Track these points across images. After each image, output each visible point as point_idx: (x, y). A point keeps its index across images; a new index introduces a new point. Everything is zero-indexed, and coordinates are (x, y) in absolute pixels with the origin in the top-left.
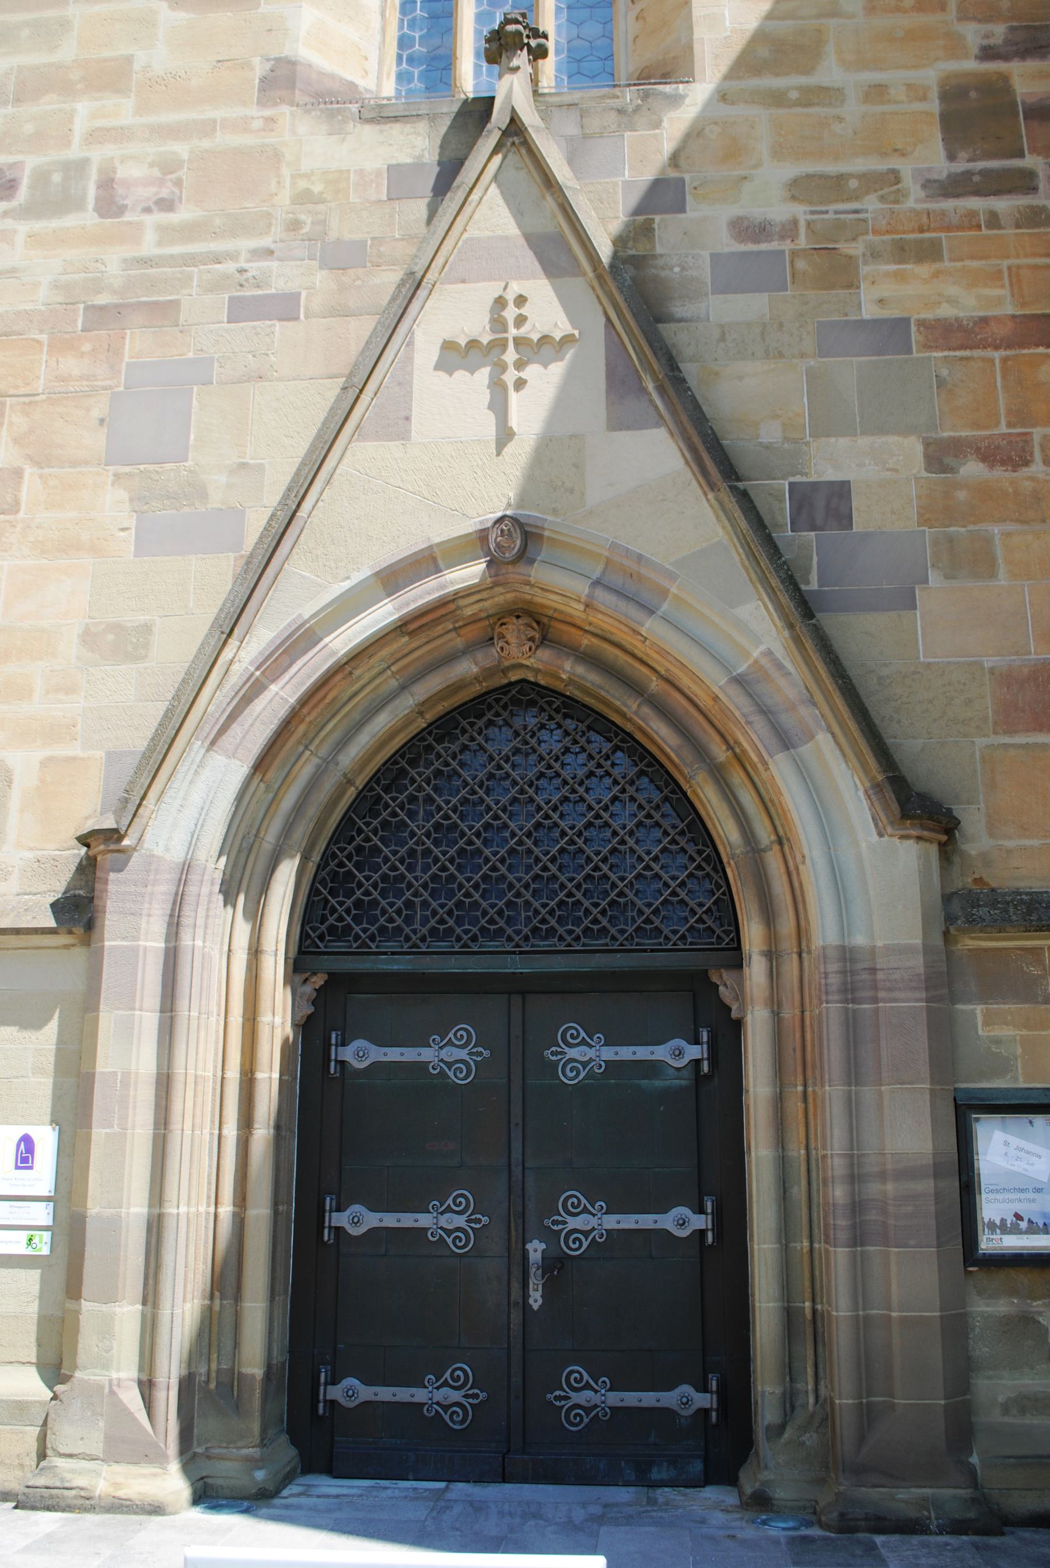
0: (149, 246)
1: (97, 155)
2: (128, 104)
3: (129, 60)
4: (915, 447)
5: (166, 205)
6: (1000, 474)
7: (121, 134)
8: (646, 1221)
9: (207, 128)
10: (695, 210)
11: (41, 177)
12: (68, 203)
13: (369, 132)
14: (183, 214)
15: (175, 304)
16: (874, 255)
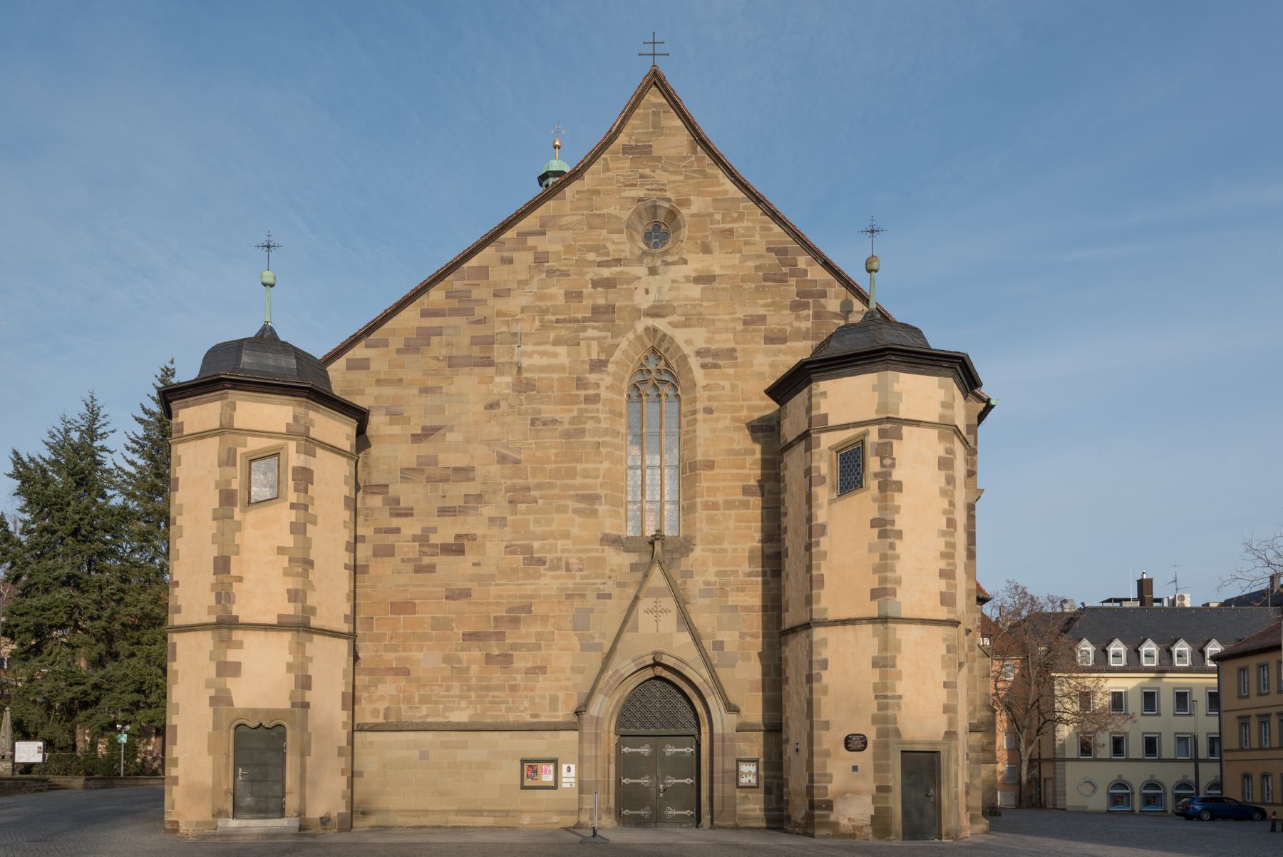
0: (578, 580)
1: (565, 555)
2: (570, 542)
3: (569, 531)
4: (737, 634)
5: (581, 570)
6: (754, 640)
7: (568, 551)
8: (682, 781)
9: (589, 551)
10: (696, 578)
11: (552, 561)
12: (558, 568)
13: (626, 554)
15: (585, 595)
16: (732, 590)
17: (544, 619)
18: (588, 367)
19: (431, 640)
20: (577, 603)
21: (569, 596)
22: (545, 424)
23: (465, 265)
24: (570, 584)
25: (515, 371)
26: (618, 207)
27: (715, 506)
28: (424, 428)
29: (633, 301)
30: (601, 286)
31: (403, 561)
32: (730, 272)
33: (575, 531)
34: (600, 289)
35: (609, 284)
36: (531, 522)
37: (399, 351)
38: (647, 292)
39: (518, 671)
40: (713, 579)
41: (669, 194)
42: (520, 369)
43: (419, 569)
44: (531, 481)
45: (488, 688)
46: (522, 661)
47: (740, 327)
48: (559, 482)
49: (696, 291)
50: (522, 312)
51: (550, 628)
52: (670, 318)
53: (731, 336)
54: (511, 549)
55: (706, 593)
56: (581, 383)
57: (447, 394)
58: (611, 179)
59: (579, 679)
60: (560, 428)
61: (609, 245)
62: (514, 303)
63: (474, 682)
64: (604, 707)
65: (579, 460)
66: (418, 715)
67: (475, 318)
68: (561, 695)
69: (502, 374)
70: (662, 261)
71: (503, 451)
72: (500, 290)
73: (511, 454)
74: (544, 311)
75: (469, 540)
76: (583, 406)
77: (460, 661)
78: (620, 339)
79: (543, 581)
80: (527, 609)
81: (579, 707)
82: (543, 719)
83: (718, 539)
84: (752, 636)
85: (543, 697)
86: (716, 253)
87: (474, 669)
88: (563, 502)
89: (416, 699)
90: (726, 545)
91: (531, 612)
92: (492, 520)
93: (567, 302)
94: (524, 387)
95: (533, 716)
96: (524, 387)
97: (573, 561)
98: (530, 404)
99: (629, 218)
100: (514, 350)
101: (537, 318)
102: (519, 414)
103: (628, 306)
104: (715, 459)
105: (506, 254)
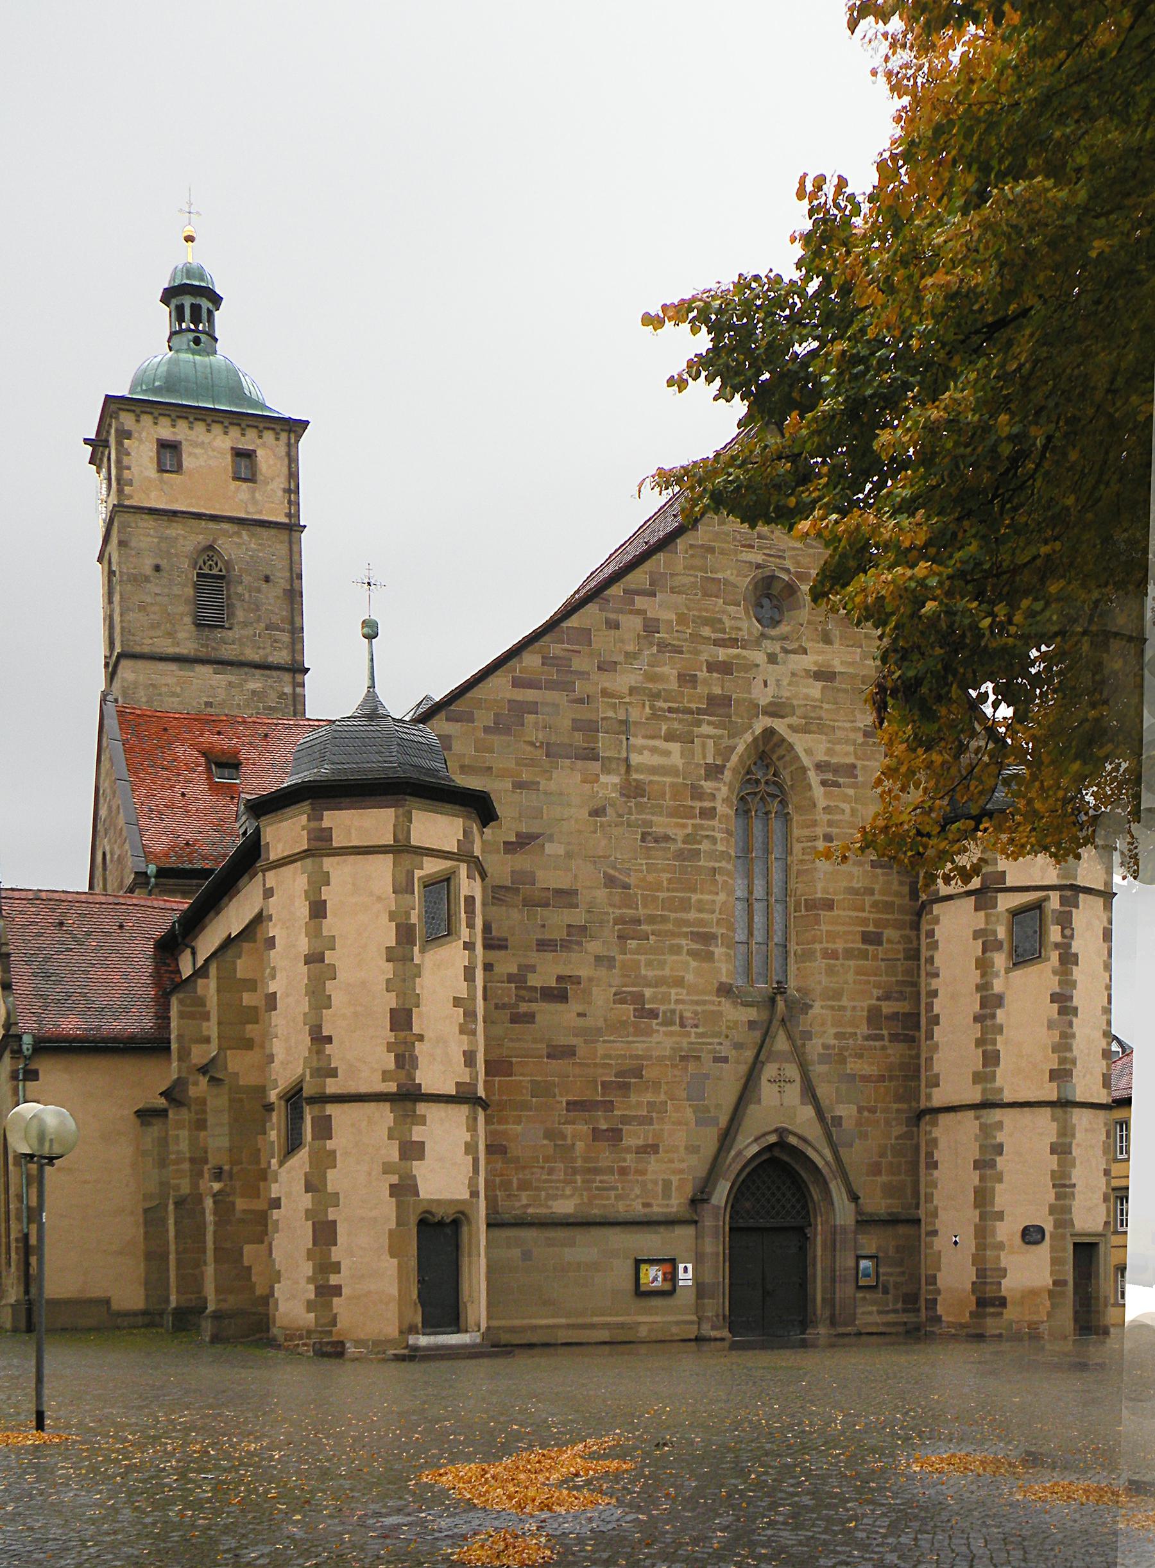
2: (685, 992)
4: (855, 1107)
5: (696, 1026)
9: (704, 1002)
11: (665, 1013)
12: (672, 1023)
14: (700, 1030)
16: (850, 1055)
17: (656, 1085)
18: (703, 772)
19: (530, 1110)
20: (691, 1066)
21: (683, 1058)
22: (656, 841)
23: (564, 625)
24: (685, 1042)
25: (623, 770)
26: (735, 572)
27: (834, 955)
28: (518, 835)
29: (750, 693)
30: (718, 671)
31: (497, 1007)
32: (851, 670)
33: (690, 977)
34: (715, 675)
35: (724, 668)
36: (643, 964)
37: (487, 730)
38: (766, 685)
39: (628, 1150)
40: (833, 1042)
41: (788, 564)
42: (628, 767)
43: (516, 1019)
44: (642, 912)
45: (596, 1171)
46: (633, 1138)
47: (860, 740)
48: (673, 915)
49: (815, 690)
50: (630, 695)
51: (663, 1097)
52: (787, 720)
53: (851, 749)
54: (620, 998)
55: (824, 1059)
56: (697, 793)
57: (546, 793)
58: (727, 535)
59: (693, 1160)
60: (673, 847)
61: (725, 619)
62: (623, 681)
63: (579, 1163)
64: (721, 1193)
65: (694, 891)
66: (517, 1204)
67: (577, 695)
68: (675, 1179)
69: (607, 770)
70: (782, 648)
71: (612, 872)
72: (604, 662)
73: (621, 877)
74: (656, 696)
75: (573, 983)
76: (698, 821)
77: (564, 1137)
78: (737, 740)
79: (656, 1038)
80: (638, 1072)
81: (695, 1195)
82: (656, 1209)
83: (837, 995)
84: (872, 1110)
85: (655, 1182)
86: (836, 646)
87: (580, 1145)
88: (675, 941)
89: (515, 1186)
90: (845, 1002)
91: (641, 1077)
92: (598, 959)
93: (680, 687)
94: (633, 791)
95: (646, 1205)
96: (633, 791)
97: (688, 1014)
98: (638, 813)
99: (747, 588)
100: (621, 742)
101: (647, 703)
102: (629, 826)
103: (745, 700)
104: (836, 898)
105: (612, 616)
